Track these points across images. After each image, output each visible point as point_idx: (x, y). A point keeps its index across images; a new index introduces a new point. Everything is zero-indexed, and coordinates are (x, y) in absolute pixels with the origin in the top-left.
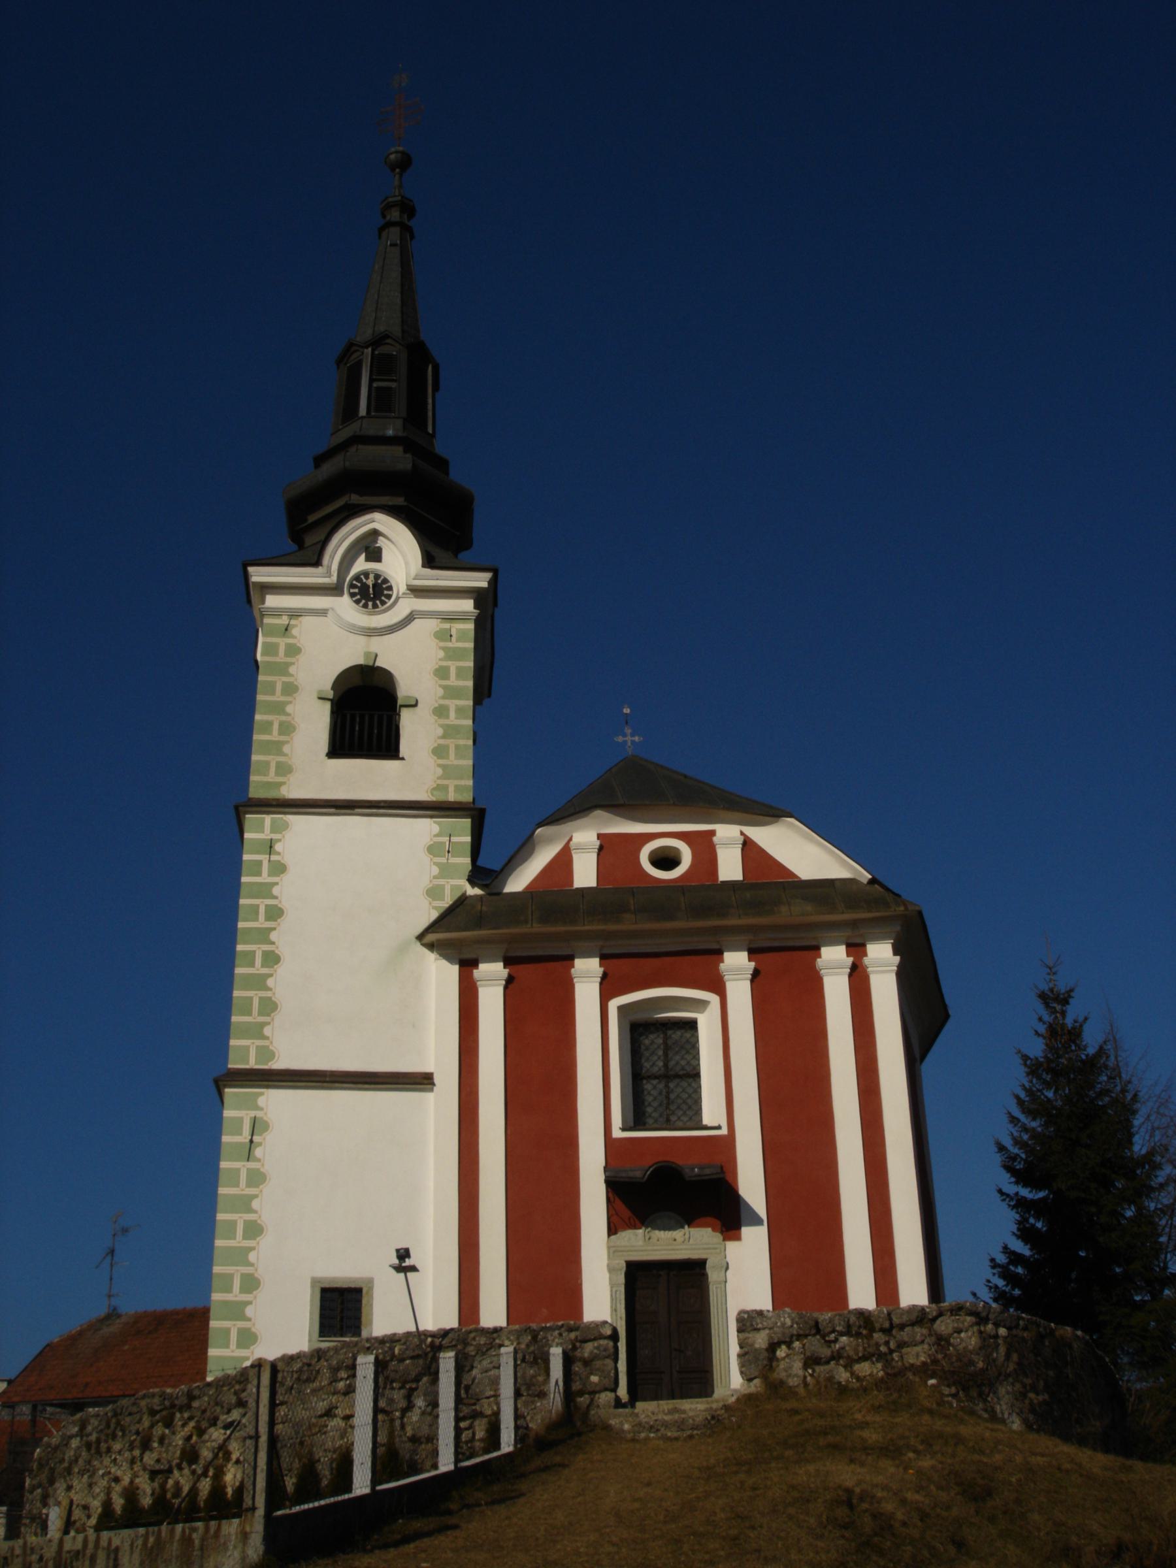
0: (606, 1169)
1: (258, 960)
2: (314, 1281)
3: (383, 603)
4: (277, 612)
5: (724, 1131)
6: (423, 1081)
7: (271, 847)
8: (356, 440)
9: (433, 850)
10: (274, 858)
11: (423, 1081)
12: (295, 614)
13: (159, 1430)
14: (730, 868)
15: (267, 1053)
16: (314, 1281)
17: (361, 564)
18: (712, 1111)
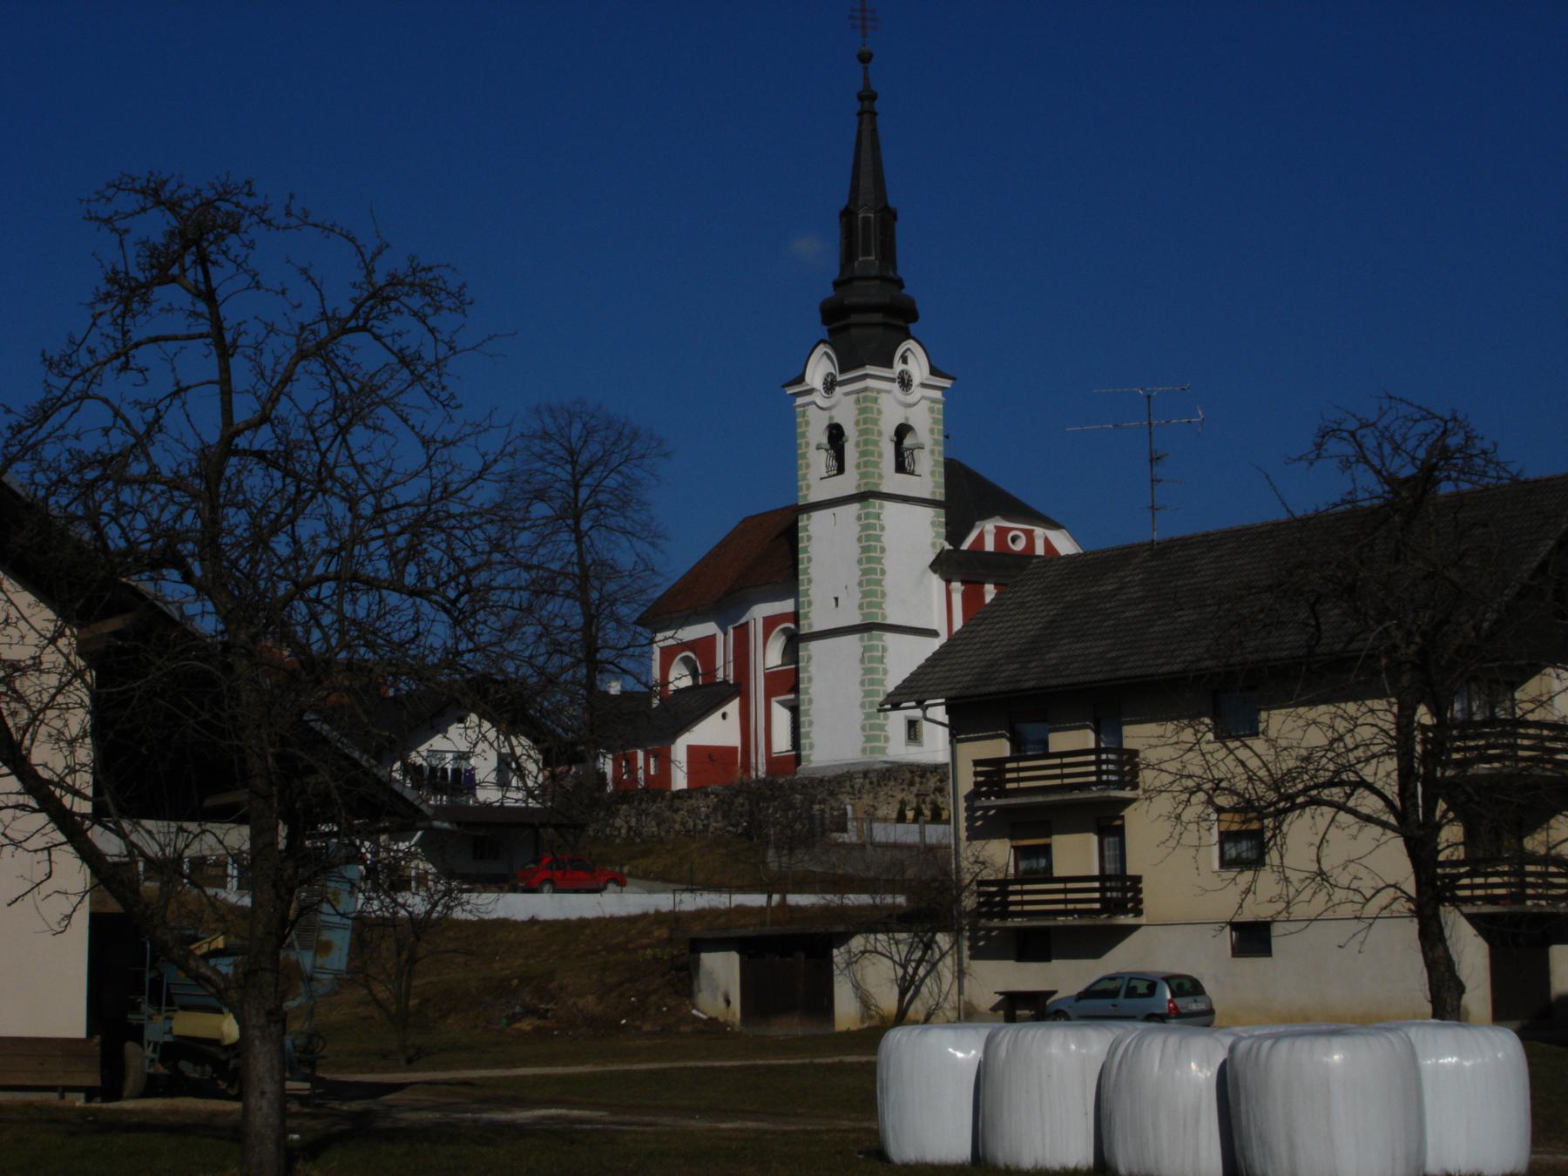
12: (879, 391)
13: (917, 779)
14: (1040, 550)
15: (884, 617)
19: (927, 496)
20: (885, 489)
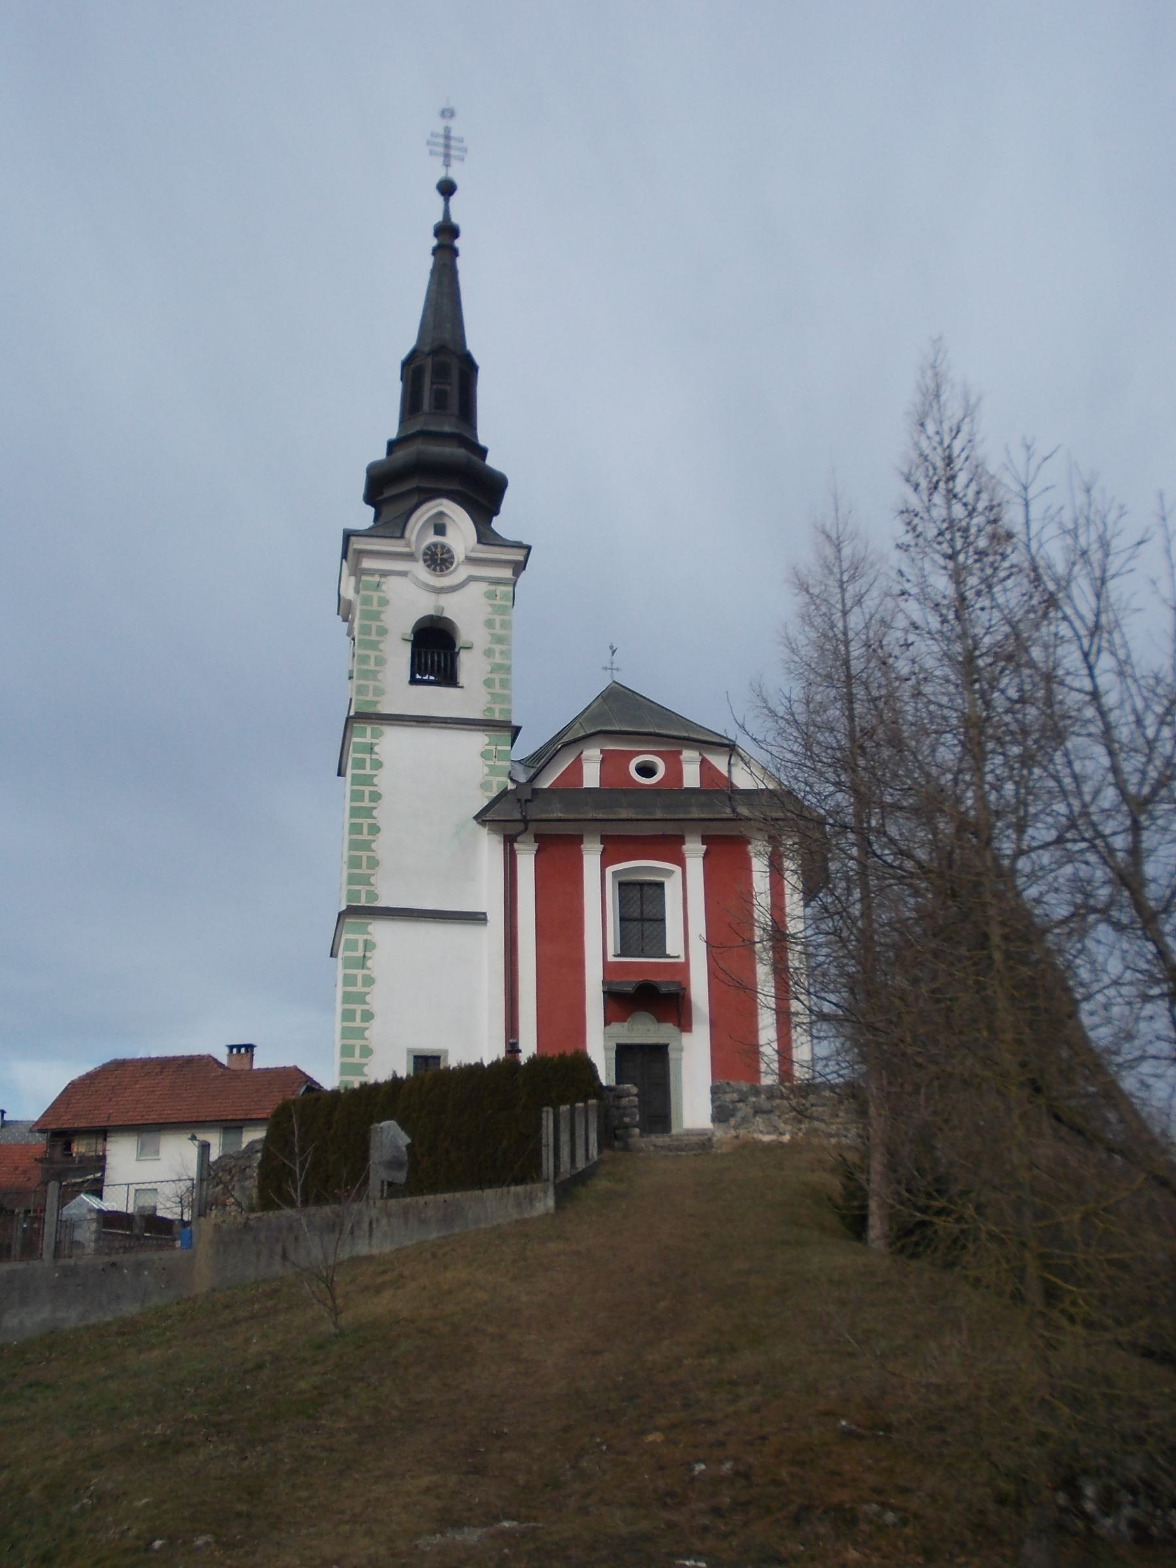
0: (603, 982)
1: (365, 830)
2: (409, 1051)
3: (447, 568)
4: (371, 572)
5: (682, 960)
6: (478, 918)
7: (371, 749)
8: (424, 434)
9: (485, 755)
10: (374, 756)
11: (478, 918)
12: (385, 574)
14: (691, 777)
15: (373, 896)
16: (409, 1051)
17: (432, 538)
18: (673, 945)
19: (477, 715)
20: (385, 709)
